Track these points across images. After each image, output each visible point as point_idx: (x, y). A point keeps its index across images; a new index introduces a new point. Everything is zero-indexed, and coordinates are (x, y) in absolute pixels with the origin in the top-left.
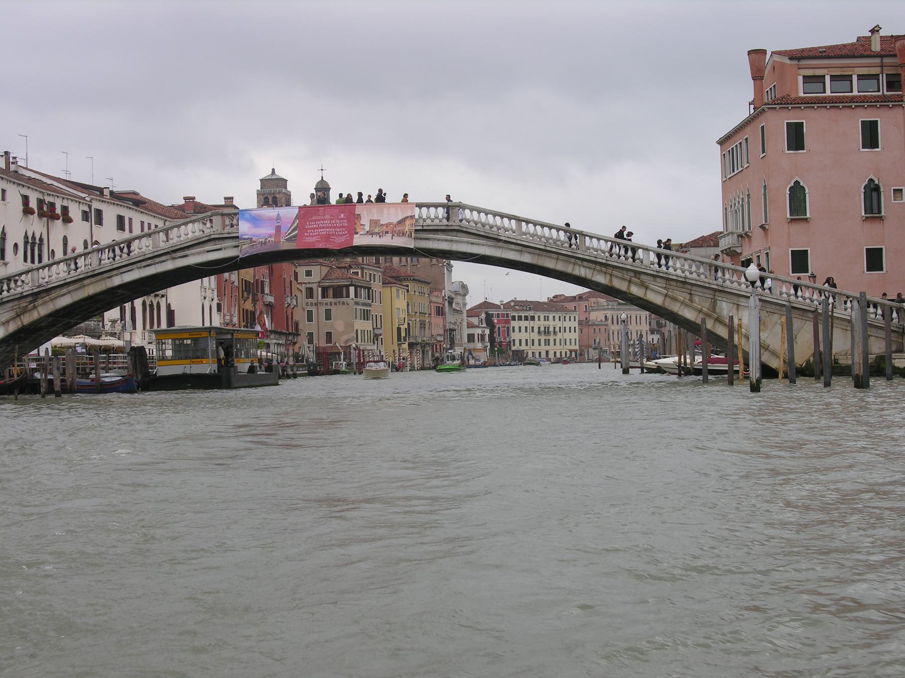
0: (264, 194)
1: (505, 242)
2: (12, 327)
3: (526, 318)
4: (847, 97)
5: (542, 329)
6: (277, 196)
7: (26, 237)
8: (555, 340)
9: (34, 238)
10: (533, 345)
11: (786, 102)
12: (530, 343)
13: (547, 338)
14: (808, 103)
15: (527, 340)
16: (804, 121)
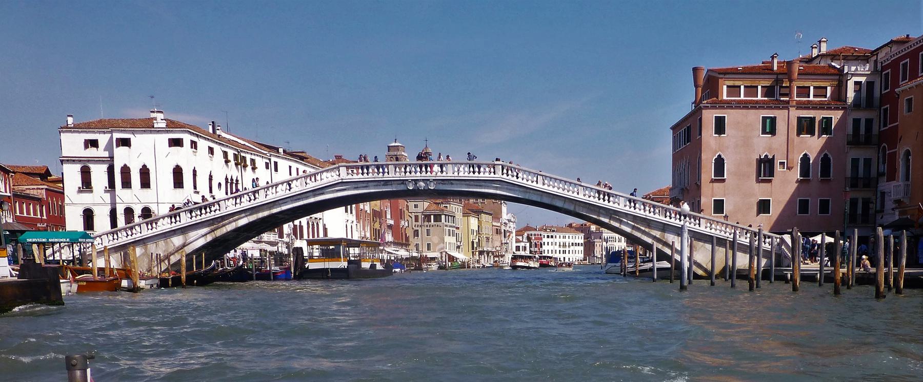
2: (209, 238)
3: (552, 237)
4: (754, 100)
5: (562, 244)
7: (227, 179)
8: (569, 251)
9: (232, 179)
10: (556, 253)
12: (554, 252)
13: (564, 249)
14: (729, 104)
15: (552, 250)
16: (726, 115)
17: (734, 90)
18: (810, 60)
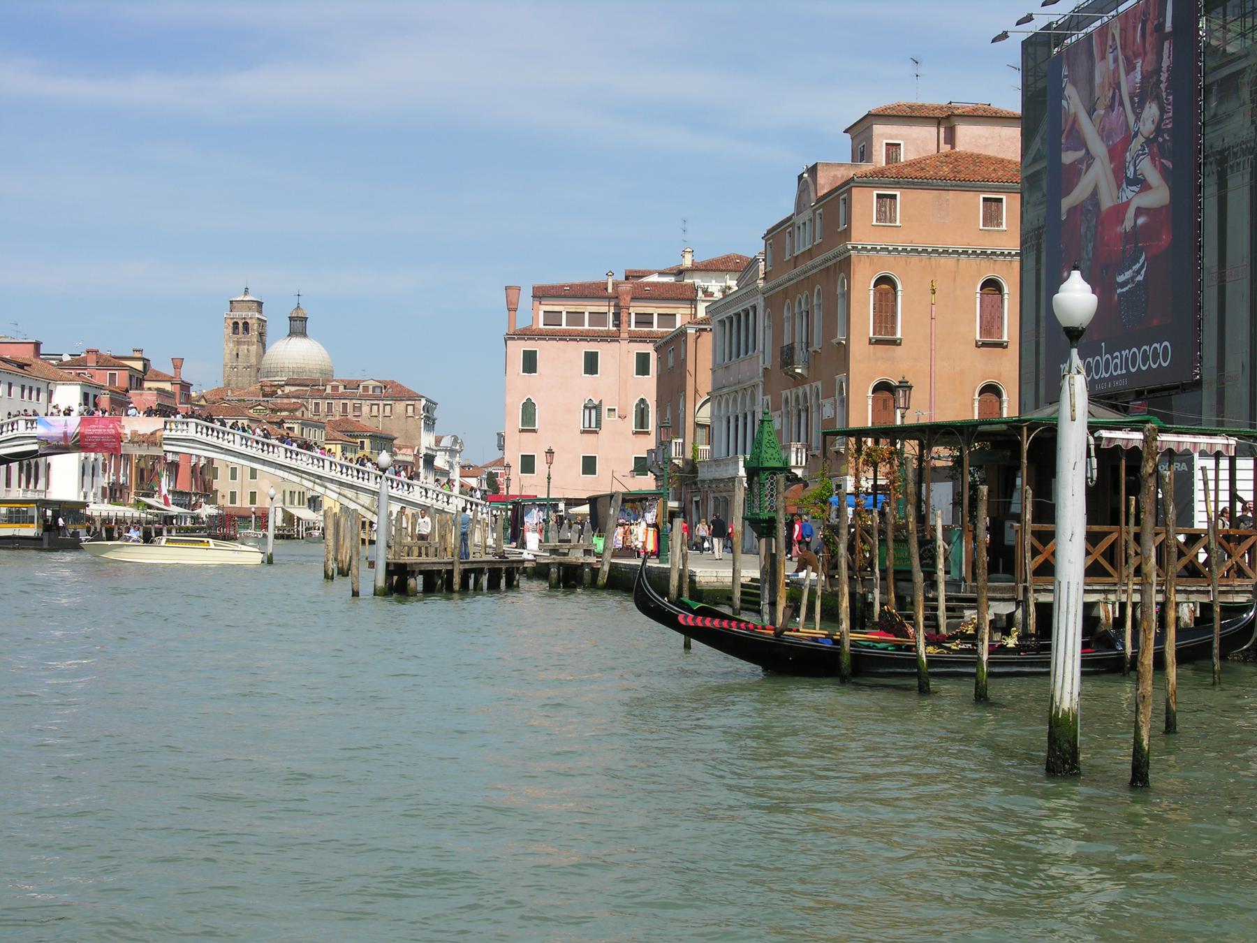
0: (234, 318)
1: (227, 450)
6: (247, 321)
11: (528, 334)
17: (552, 317)
18: (680, 273)
